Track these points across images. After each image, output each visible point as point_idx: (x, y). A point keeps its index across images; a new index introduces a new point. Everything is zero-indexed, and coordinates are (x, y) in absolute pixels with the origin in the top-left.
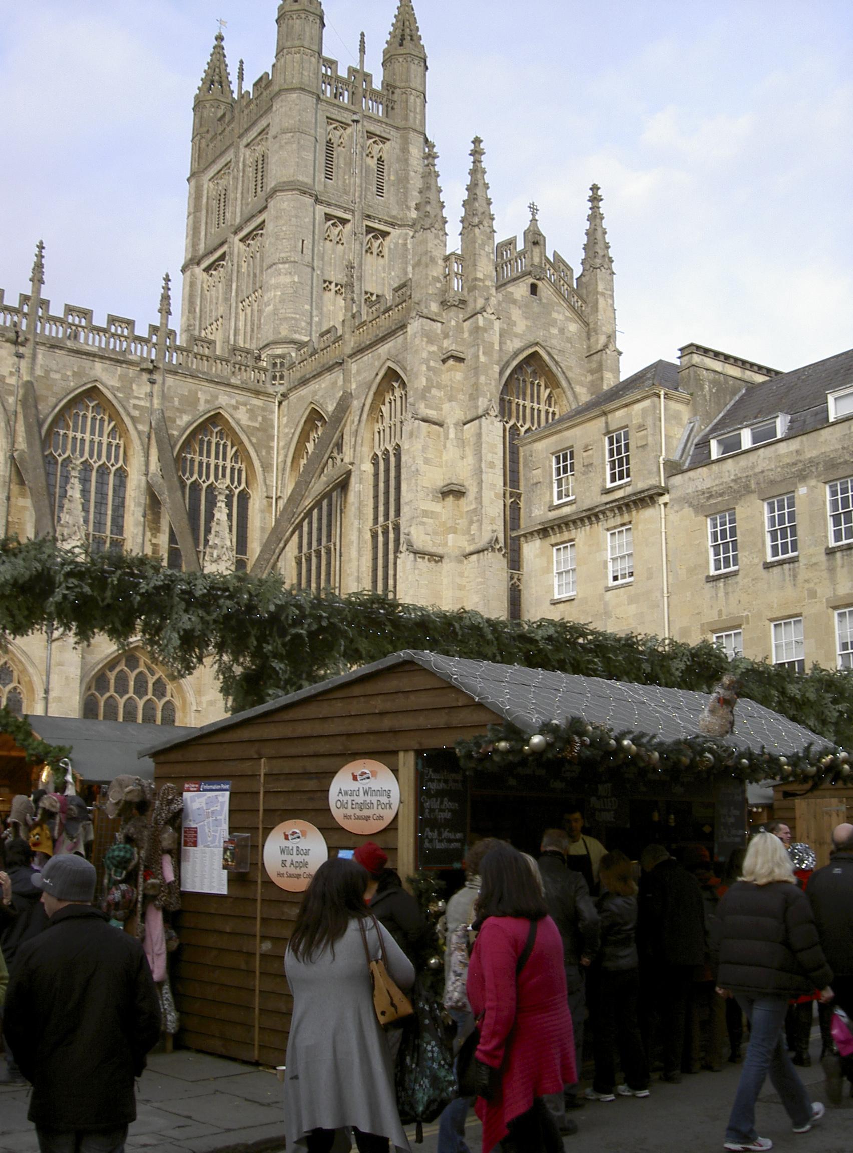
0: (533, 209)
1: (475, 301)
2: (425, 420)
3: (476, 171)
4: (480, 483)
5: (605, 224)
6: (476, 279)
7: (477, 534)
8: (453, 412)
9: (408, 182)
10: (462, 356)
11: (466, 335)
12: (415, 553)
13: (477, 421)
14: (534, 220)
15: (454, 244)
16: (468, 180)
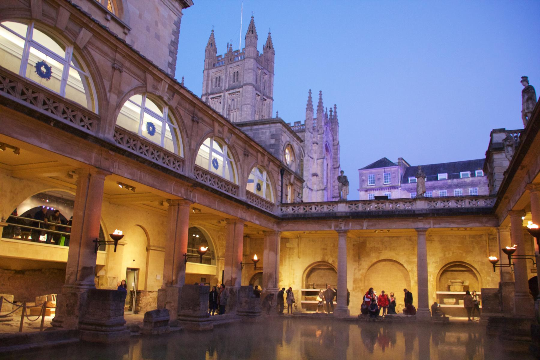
0: (326, 108)
1: (321, 131)
2: (311, 157)
3: (321, 99)
4: (323, 175)
5: (337, 114)
6: (322, 126)
7: (322, 186)
8: (315, 156)
9: (271, 87)
10: (318, 143)
11: (318, 138)
12: (309, 189)
13: (322, 160)
14: (326, 112)
15: (315, 116)
16: (318, 101)
